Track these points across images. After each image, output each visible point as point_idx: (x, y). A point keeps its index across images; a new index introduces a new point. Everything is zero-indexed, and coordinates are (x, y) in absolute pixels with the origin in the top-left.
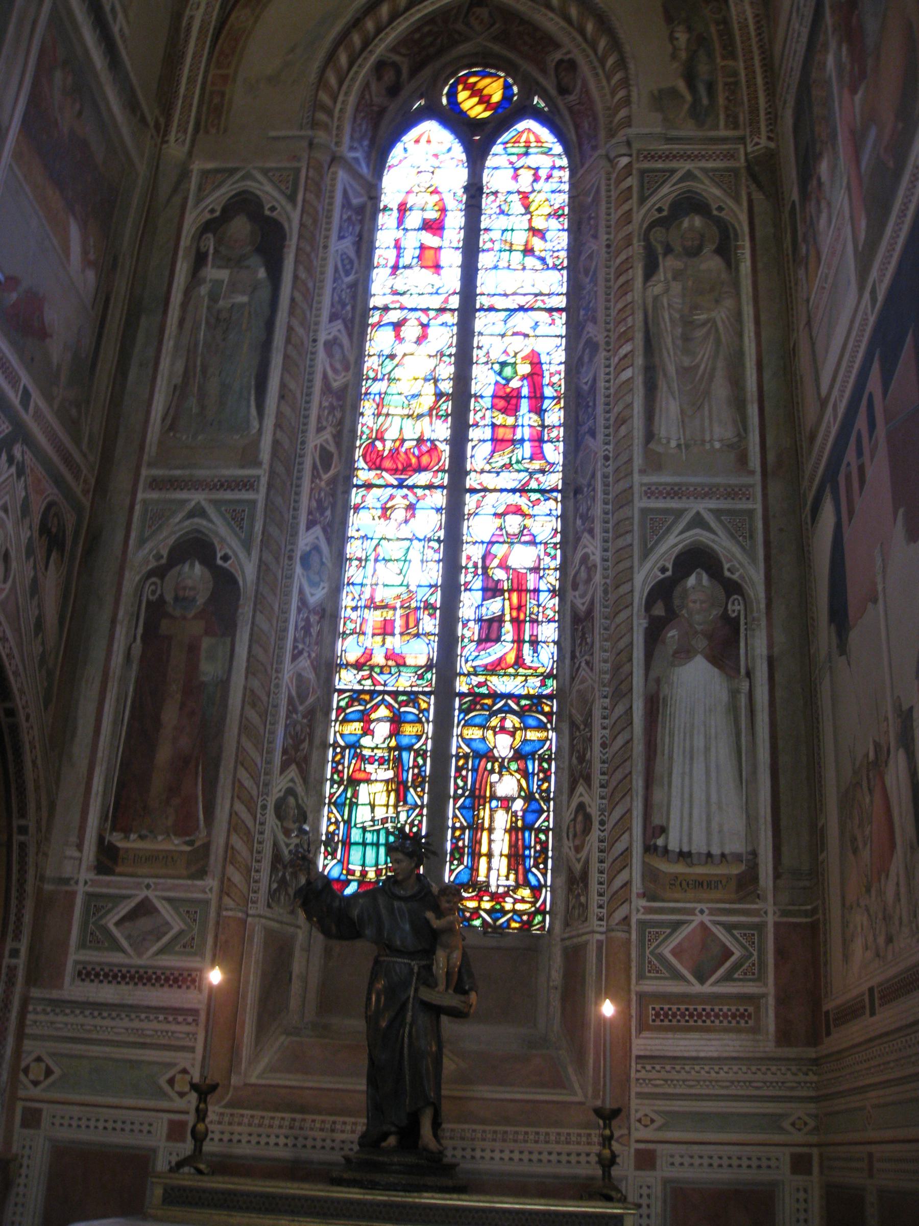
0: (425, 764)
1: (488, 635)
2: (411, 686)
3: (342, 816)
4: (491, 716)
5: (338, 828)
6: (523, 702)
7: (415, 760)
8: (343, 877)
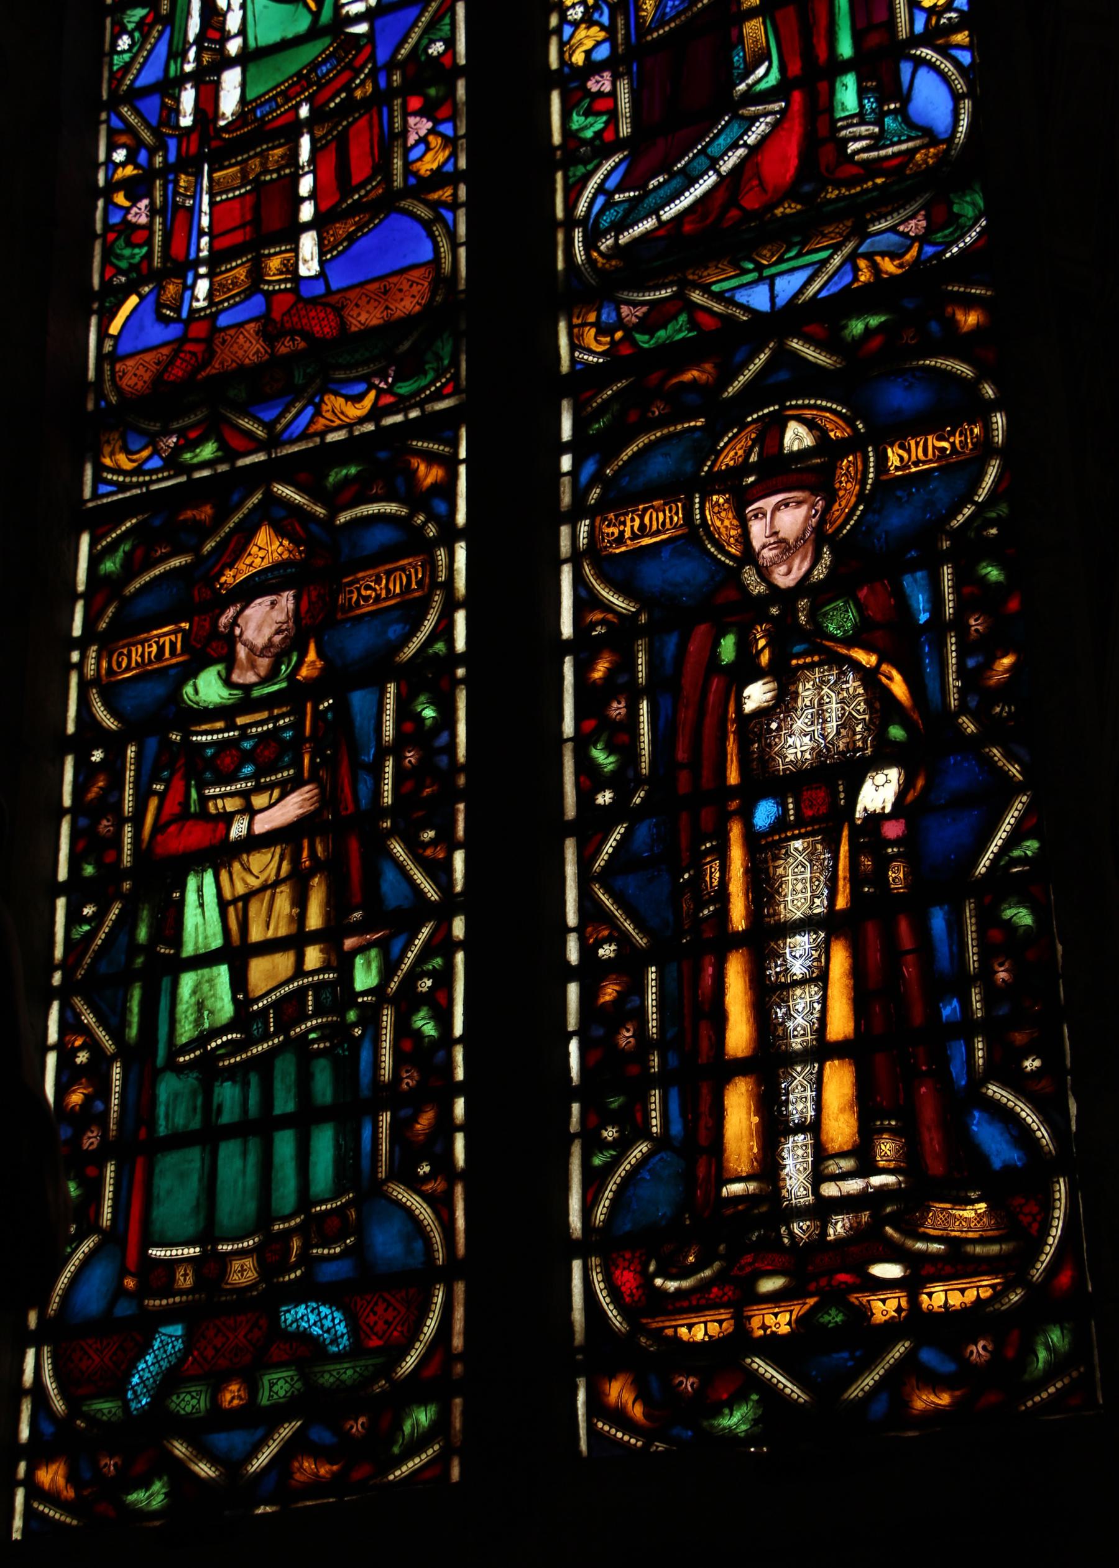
2: (375, 414)
4: (713, 432)
5: (104, 1091)
7: (404, 712)
8: (124, 1309)
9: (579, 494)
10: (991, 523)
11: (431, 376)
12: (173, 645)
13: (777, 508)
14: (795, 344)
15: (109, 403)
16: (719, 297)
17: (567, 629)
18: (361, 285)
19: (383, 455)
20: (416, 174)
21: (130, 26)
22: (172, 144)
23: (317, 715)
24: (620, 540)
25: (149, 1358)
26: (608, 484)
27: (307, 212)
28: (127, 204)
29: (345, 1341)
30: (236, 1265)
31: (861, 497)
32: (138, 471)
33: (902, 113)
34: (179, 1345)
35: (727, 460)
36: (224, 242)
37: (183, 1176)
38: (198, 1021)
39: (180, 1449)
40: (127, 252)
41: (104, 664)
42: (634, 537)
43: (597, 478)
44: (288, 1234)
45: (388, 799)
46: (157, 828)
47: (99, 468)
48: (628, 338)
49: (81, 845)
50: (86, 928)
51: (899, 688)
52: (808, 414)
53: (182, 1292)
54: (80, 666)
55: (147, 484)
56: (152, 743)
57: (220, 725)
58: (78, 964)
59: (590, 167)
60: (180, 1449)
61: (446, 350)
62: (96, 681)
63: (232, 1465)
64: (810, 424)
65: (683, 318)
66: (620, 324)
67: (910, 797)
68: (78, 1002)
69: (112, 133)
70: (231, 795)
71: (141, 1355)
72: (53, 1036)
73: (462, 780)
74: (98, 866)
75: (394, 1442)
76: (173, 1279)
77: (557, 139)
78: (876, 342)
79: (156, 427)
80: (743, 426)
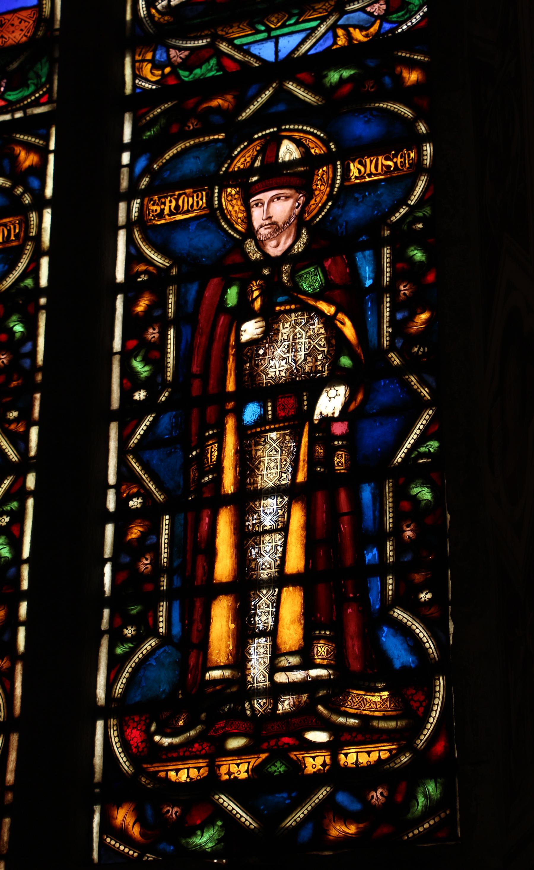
6: (334, 77)
13: (271, 200)
14: (291, 86)
17: (120, 276)
24: (161, 215)
26: (154, 175)
31: (330, 196)
35: (239, 164)
42: (171, 214)
52: (297, 135)
64: (298, 143)
65: (213, 62)
73: (39, 377)
78: (346, 89)
80: (251, 141)
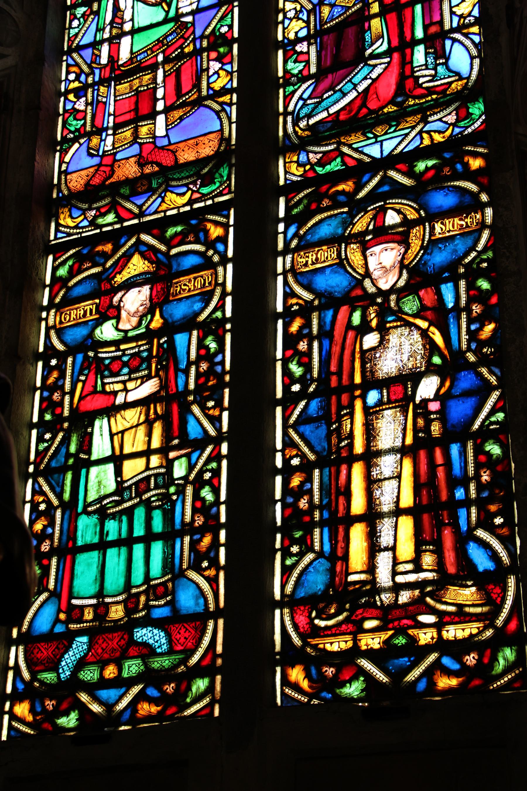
0: (221, 349)
1: (336, 57)
2: (190, 202)
3: (59, 496)
4: (352, 215)
5: (52, 523)
6: (421, 166)
7: (201, 345)
8: (59, 629)
9: (287, 244)
10: (484, 261)
11: (218, 184)
12: (91, 310)
13: (381, 251)
15: (63, 195)
16: (356, 150)
18: (185, 141)
19: (193, 222)
20: (212, 89)
21: (79, 16)
22: (97, 72)
23: (160, 345)
24: (306, 265)
25: (71, 653)
26: (301, 238)
27: (160, 106)
28: (75, 100)
29: (165, 647)
30: (113, 608)
31: (422, 248)
32: (77, 227)
33: (446, 64)
34: (85, 647)
35: (359, 227)
36: (120, 120)
37: (89, 565)
38: (98, 491)
39: (84, 697)
40: (74, 123)
41: (58, 319)
42: (313, 263)
43: (296, 235)
44: (138, 594)
45: (192, 386)
46: (81, 398)
47: (58, 225)
48: (312, 169)
49: (45, 405)
50: (46, 444)
51: (438, 339)
52: (397, 206)
53: (87, 621)
54: (46, 319)
55: (80, 233)
56: (80, 357)
57: (113, 349)
58: (41, 462)
59: (296, 87)
60: (84, 697)
61: (225, 173)
62: (54, 327)
63: (109, 706)
64: (399, 212)
65: (339, 160)
66: (309, 162)
67: (442, 391)
68: (41, 480)
69: (68, 66)
70: (117, 382)
71: (66, 651)
72: (28, 497)
74: (53, 414)
75: (187, 696)
76: (83, 614)
77: (280, 74)
78: (431, 174)
79: (85, 206)
80: (366, 212)
